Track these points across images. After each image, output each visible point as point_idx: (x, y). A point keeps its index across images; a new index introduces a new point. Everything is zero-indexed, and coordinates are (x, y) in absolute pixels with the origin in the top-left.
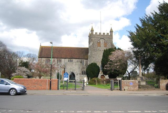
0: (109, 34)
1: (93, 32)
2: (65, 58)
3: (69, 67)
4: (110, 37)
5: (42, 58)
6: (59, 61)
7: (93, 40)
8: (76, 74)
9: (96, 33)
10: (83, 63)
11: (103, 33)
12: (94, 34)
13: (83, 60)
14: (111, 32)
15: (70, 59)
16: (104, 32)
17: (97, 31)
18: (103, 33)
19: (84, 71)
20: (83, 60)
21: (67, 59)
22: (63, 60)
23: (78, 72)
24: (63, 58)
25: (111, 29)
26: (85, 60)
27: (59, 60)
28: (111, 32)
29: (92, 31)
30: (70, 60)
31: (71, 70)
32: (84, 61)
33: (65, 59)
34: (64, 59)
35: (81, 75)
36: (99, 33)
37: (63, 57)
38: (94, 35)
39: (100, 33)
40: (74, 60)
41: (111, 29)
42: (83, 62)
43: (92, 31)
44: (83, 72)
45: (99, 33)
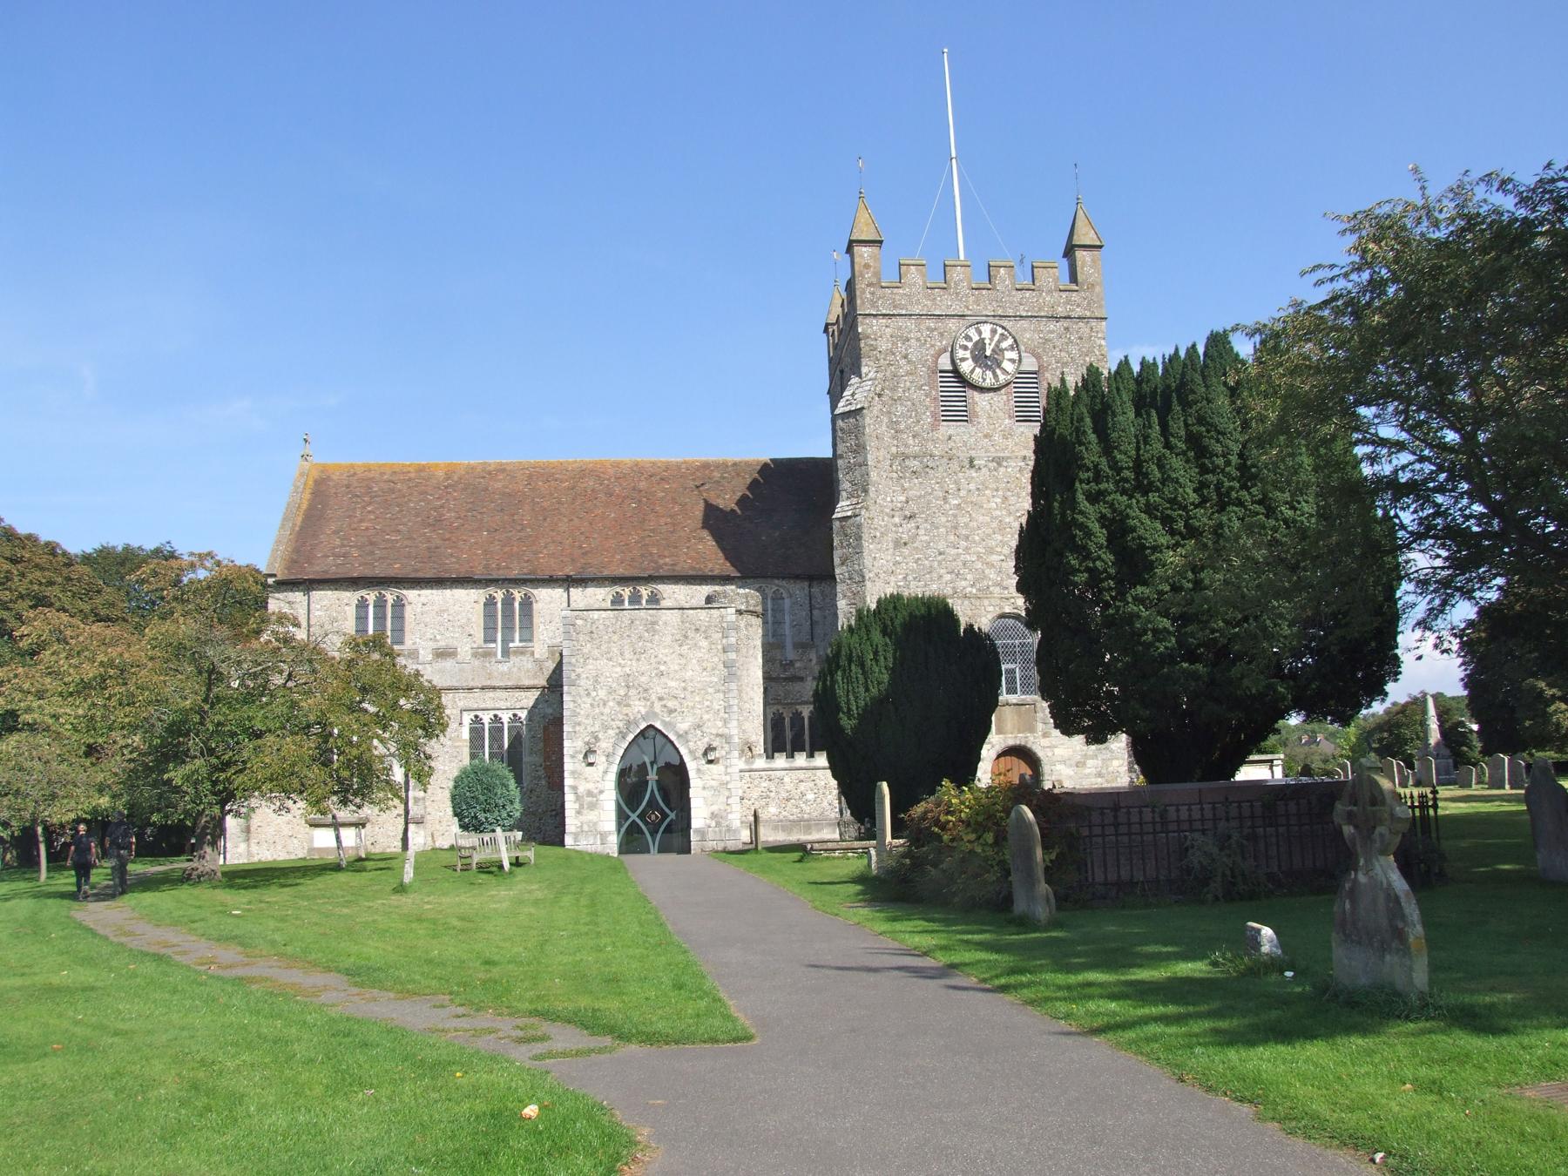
2: (569, 582)
3: (612, 672)
4: (1068, 302)
5: (308, 585)
7: (884, 345)
8: (702, 747)
15: (626, 592)
19: (797, 717)
22: (548, 600)
24: (550, 581)
27: (509, 601)
30: (636, 599)
31: (638, 707)
34: (558, 593)
40: (674, 594)
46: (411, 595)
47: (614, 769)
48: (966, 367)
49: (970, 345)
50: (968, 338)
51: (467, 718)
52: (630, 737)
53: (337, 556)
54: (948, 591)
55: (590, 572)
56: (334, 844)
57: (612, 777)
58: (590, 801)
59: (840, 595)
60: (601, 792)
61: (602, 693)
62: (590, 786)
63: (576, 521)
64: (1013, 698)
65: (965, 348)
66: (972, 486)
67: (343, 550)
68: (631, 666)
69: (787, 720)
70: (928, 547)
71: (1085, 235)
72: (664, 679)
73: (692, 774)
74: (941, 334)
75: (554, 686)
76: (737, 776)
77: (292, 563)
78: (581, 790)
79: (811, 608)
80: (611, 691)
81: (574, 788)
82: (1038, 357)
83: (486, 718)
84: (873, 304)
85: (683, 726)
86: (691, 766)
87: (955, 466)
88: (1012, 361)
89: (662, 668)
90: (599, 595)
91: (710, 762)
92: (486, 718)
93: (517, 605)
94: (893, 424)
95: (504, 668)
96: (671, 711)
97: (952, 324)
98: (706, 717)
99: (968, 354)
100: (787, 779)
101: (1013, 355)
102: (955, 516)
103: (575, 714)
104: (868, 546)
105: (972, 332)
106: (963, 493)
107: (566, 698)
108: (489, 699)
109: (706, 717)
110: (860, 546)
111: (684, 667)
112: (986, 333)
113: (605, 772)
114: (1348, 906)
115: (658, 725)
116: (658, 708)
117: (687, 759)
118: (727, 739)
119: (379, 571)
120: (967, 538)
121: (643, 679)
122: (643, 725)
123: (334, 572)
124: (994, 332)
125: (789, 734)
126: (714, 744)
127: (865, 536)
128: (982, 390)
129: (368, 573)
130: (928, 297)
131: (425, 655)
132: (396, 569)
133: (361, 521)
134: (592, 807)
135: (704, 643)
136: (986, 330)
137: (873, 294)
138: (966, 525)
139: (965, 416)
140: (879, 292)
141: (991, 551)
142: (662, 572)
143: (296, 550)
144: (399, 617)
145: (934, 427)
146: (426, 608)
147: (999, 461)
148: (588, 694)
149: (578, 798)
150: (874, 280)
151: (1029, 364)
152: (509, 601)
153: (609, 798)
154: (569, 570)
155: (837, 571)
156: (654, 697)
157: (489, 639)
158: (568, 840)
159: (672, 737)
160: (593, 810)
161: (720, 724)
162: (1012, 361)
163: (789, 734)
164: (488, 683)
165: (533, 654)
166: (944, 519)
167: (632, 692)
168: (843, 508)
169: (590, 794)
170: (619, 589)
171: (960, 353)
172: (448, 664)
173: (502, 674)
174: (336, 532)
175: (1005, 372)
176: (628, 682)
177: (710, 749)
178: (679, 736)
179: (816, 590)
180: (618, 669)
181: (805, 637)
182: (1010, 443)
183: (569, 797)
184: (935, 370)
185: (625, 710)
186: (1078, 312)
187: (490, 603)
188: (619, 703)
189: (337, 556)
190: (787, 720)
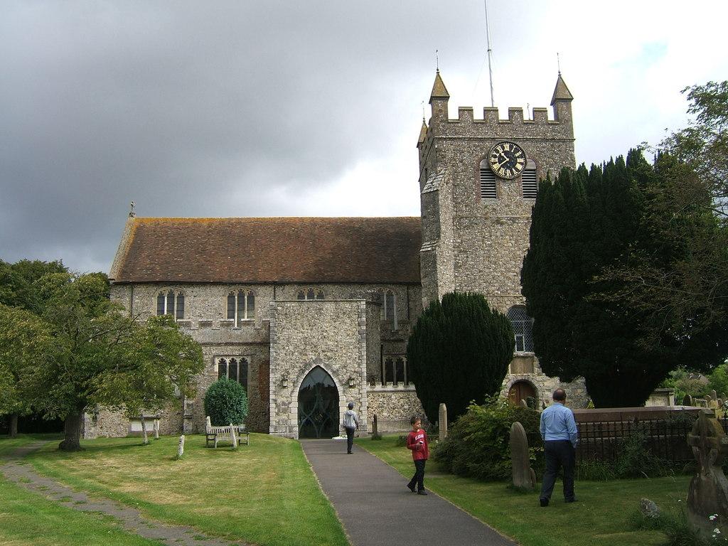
0: (551, 117)
1: (446, 107)
2: (275, 284)
3: (297, 336)
4: (553, 130)
5: (132, 285)
6: (241, 303)
7: (450, 155)
8: (346, 378)
9: (466, 111)
10: (390, 309)
11: (512, 111)
12: (453, 114)
13: (390, 295)
14: (562, 99)
15: (306, 289)
16: (515, 105)
17: (469, 95)
18: (512, 111)
19: (400, 362)
20: (390, 295)
21: (287, 288)
23: (353, 367)
24: (265, 284)
25: (561, 85)
26: (399, 294)
27: (241, 296)
28: (562, 99)
29: (439, 98)
31: (312, 356)
32: (395, 298)
33: (279, 290)
34: (269, 290)
35: (379, 387)
36: (486, 111)
37: (262, 276)
38: (455, 122)
39: (490, 111)
41: (561, 85)
42: (390, 302)
43: (439, 98)
44: (389, 364)
45: (486, 111)
46: (188, 291)
47: (298, 390)
49: (498, 155)
50: (497, 151)
51: (217, 361)
52: (307, 372)
53: (148, 269)
54: (484, 292)
55: (287, 279)
56: (142, 430)
57: (296, 394)
58: (284, 408)
59: (423, 295)
60: (290, 403)
61: (291, 348)
62: (285, 399)
63: (279, 252)
64: (521, 353)
65: (495, 157)
66: (498, 234)
67: (151, 267)
68: (308, 333)
69: (394, 363)
70: (473, 268)
72: (326, 340)
73: (340, 393)
74: (482, 149)
75: (265, 344)
76: (365, 395)
77: (123, 272)
78: (279, 401)
79: (409, 301)
80: (296, 347)
81: (275, 400)
82: (536, 161)
83: (228, 361)
84: (444, 133)
85: (336, 367)
86: (340, 389)
87: (488, 222)
88: (521, 164)
89: (325, 334)
90: (291, 291)
91: (351, 387)
92: (228, 361)
93: (246, 297)
94: (454, 199)
95: (238, 332)
96: (329, 358)
98: (348, 362)
100: (393, 397)
101: (521, 160)
102: (488, 251)
103: (276, 359)
104: (440, 267)
105: (499, 148)
106: (493, 238)
107: (271, 350)
108: (229, 350)
109: (348, 362)
110: (435, 268)
111: (337, 334)
112: (507, 149)
113: (292, 392)
114: (695, 493)
115: (322, 366)
116: (322, 356)
118: (360, 374)
119: (170, 279)
120: (495, 263)
121: (314, 340)
122: (314, 366)
123: (146, 278)
124: (511, 147)
125: (395, 372)
126: (353, 377)
127: (438, 262)
128: (504, 179)
129: (164, 279)
130: (474, 128)
131: (195, 325)
132: (180, 277)
133: (161, 250)
134: (285, 411)
135: (348, 321)
136: (507, 147)
137: (443, 126)
138: (495, 255)
139: (495, 195)
140: (448, 126)
141: (509, 270)
142: (326, 280)
143: (125, 266)
144: (181, 304)
145: (477, 201)
146: (196, 299)
147: (514, 220)
148: (284, 348)
149: (277, 406)
150: (445, 119)
151: (531, 165)
152: (241, 296)
153: (294, 407)
154: (275, 279)
155: (422, 281)
156: (320, 350)
157: (231, 316)
159: (330, 373)
160: (285, 409)
161: (356, 366)
162: (521, 164)
163: (395, 372)
164: (229, 341)
165: (254, 325)
166: (482, 252)
167: (308, 347)
168: (426, 247)
169: (284, 403)
172: (208, 330)
173: (238, 336)
174: (148, 256)
175: (517, 170)
176: (306, 341)
177: (351, 379)
178: (334, 372)
179: (411, 291)
180: (301, 334)
181: (405, 317)
182: (520, 210)
183: (272, 405)
185: (304, 357)
186: (559, 136)
187: (231, 297)
188: (301, 354)
189: (148, 269)
190: (394, 363)
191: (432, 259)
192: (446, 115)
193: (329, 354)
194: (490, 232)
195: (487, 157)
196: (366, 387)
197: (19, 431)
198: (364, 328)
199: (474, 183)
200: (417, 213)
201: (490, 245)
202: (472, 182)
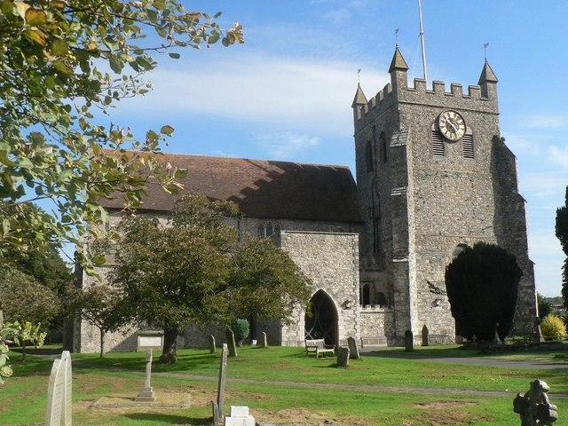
4: (484, 105)
7: (409, 117)
16: (456, 82)
23: (348, 291)
48: (444, 130)
65: (443, 122)
66: (447, 185)
71: (490, 77)
76: (359, 315)
82: (473, 129)
85: (335, 291)
86: (339, 309)
91: (347, 308)
97: (437, 110)
99: (444, 125)
117: (337, 306)
118: (355, 298)
132: (153, 206)
139: (443, 153)
145: (430, 157)
147: (458, 175)
151: (469, 131)
158: (283, 344)
159: (330, 295)
167: (313, 273)
170: (261, 222)
171: (441, 124)
177: (347, 302)
184: (429, 130)
186: (488, 110)
191: (401, 203)
192: (406, 83)
193: (329, 280)
194: (441, 183)
195: (437, 122)
196: (360, 309)
197: (269, 344)
198: (357, 258)
199: (428, 142)
200: (347, 159)
201: (441, 194)
202: (428, 140)
